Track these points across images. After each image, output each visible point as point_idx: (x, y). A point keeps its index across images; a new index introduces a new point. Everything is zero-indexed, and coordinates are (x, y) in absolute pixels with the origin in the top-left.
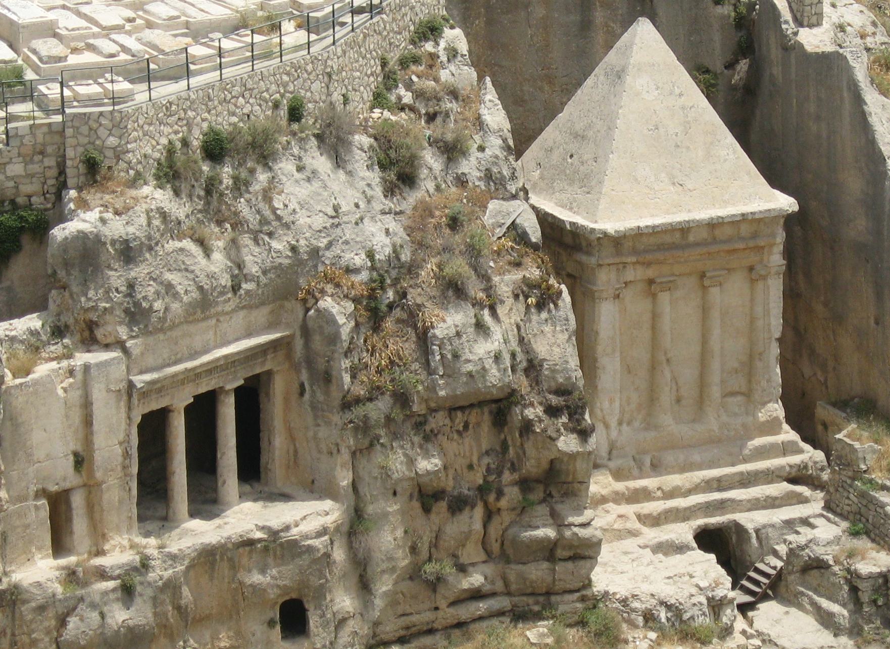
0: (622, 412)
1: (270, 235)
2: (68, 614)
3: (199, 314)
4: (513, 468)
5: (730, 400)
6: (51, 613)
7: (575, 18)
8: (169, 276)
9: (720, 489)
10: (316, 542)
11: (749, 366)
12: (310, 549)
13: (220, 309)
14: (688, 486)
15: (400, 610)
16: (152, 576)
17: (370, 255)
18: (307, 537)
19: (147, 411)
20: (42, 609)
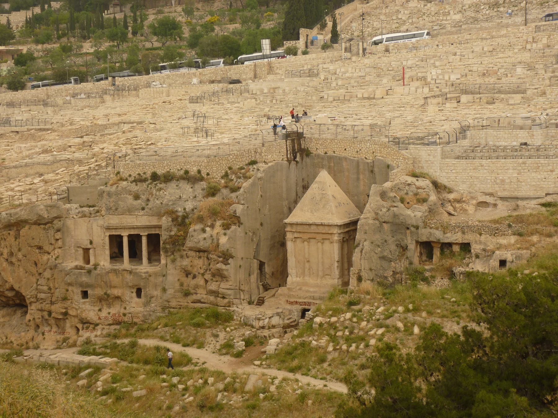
0: (297, 273)
1: (157, 199)
2: (68, 274)
3: (127, 213)
4: (210, 270)
5: (327, 276)
6: (63, 273)
7: (355, 176)
8: (120, 202)
9: (314, 299)
10: (143, 275)
11: (330, 268)
12: (141, 276)
13: (136, 214)
14: (305, 297)
15: (178, 300)
16: (96, 272)
17: (185, 209)
18: (141, 273)
19: (111, 234)
20: (61, 271)
